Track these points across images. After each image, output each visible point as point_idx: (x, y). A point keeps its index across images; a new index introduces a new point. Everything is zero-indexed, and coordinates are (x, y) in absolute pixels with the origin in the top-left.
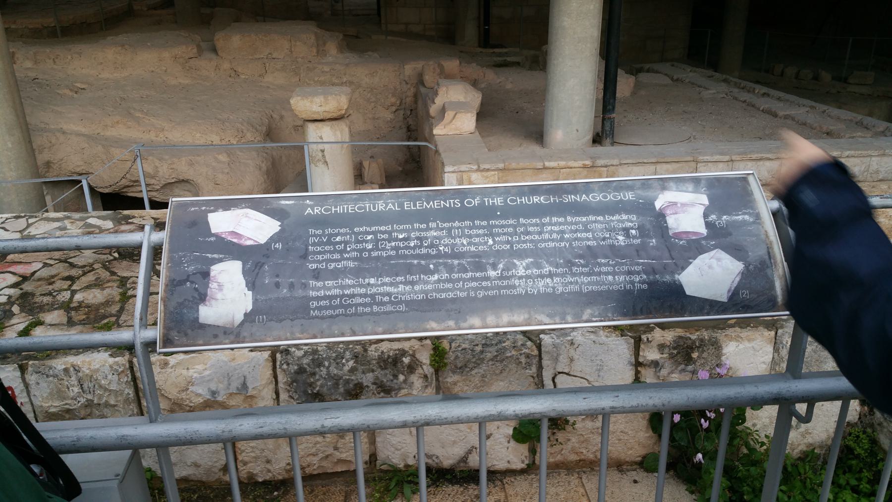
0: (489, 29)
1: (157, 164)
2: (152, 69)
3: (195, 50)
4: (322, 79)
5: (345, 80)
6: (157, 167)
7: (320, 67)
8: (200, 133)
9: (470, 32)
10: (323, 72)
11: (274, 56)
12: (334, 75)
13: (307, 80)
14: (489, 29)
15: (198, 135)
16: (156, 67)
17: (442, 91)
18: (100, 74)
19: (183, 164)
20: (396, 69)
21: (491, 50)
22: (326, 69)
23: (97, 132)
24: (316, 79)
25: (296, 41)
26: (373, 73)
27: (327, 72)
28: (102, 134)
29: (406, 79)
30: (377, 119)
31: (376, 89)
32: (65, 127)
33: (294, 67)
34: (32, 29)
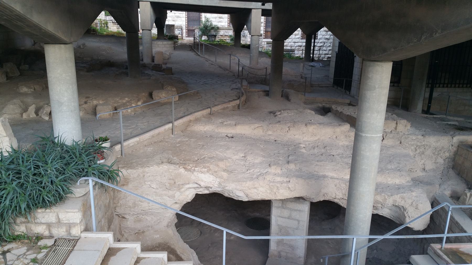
1: (386, 198)
2: (330, 136)
3: (349, 127)
4: (412, 143)
5: (424, 143)
6: (386, 199)
7: (411, 137)
8: (391, 178)
9: (420, 106)
10: (412, 139)
11: (386, 131)
12: (419, 141)
13: (405, 144)
14: (430, 106)
15: (390, 179)
16: (331, 136)
18: (304, 138)
19: (398, 197)
20: (449, 139)
21: (432, 116)
22: (414, 138)
23: (342, 177)
24: (410, 143)
25: (399, 124)
26: (438, 141)
27: (414, 140)
28: (344, 178)
29: (453, 144)
30: (437, 163)
31: (438, 148)
32: (327, 174)
33: (398, 137)
34: (233, 106)
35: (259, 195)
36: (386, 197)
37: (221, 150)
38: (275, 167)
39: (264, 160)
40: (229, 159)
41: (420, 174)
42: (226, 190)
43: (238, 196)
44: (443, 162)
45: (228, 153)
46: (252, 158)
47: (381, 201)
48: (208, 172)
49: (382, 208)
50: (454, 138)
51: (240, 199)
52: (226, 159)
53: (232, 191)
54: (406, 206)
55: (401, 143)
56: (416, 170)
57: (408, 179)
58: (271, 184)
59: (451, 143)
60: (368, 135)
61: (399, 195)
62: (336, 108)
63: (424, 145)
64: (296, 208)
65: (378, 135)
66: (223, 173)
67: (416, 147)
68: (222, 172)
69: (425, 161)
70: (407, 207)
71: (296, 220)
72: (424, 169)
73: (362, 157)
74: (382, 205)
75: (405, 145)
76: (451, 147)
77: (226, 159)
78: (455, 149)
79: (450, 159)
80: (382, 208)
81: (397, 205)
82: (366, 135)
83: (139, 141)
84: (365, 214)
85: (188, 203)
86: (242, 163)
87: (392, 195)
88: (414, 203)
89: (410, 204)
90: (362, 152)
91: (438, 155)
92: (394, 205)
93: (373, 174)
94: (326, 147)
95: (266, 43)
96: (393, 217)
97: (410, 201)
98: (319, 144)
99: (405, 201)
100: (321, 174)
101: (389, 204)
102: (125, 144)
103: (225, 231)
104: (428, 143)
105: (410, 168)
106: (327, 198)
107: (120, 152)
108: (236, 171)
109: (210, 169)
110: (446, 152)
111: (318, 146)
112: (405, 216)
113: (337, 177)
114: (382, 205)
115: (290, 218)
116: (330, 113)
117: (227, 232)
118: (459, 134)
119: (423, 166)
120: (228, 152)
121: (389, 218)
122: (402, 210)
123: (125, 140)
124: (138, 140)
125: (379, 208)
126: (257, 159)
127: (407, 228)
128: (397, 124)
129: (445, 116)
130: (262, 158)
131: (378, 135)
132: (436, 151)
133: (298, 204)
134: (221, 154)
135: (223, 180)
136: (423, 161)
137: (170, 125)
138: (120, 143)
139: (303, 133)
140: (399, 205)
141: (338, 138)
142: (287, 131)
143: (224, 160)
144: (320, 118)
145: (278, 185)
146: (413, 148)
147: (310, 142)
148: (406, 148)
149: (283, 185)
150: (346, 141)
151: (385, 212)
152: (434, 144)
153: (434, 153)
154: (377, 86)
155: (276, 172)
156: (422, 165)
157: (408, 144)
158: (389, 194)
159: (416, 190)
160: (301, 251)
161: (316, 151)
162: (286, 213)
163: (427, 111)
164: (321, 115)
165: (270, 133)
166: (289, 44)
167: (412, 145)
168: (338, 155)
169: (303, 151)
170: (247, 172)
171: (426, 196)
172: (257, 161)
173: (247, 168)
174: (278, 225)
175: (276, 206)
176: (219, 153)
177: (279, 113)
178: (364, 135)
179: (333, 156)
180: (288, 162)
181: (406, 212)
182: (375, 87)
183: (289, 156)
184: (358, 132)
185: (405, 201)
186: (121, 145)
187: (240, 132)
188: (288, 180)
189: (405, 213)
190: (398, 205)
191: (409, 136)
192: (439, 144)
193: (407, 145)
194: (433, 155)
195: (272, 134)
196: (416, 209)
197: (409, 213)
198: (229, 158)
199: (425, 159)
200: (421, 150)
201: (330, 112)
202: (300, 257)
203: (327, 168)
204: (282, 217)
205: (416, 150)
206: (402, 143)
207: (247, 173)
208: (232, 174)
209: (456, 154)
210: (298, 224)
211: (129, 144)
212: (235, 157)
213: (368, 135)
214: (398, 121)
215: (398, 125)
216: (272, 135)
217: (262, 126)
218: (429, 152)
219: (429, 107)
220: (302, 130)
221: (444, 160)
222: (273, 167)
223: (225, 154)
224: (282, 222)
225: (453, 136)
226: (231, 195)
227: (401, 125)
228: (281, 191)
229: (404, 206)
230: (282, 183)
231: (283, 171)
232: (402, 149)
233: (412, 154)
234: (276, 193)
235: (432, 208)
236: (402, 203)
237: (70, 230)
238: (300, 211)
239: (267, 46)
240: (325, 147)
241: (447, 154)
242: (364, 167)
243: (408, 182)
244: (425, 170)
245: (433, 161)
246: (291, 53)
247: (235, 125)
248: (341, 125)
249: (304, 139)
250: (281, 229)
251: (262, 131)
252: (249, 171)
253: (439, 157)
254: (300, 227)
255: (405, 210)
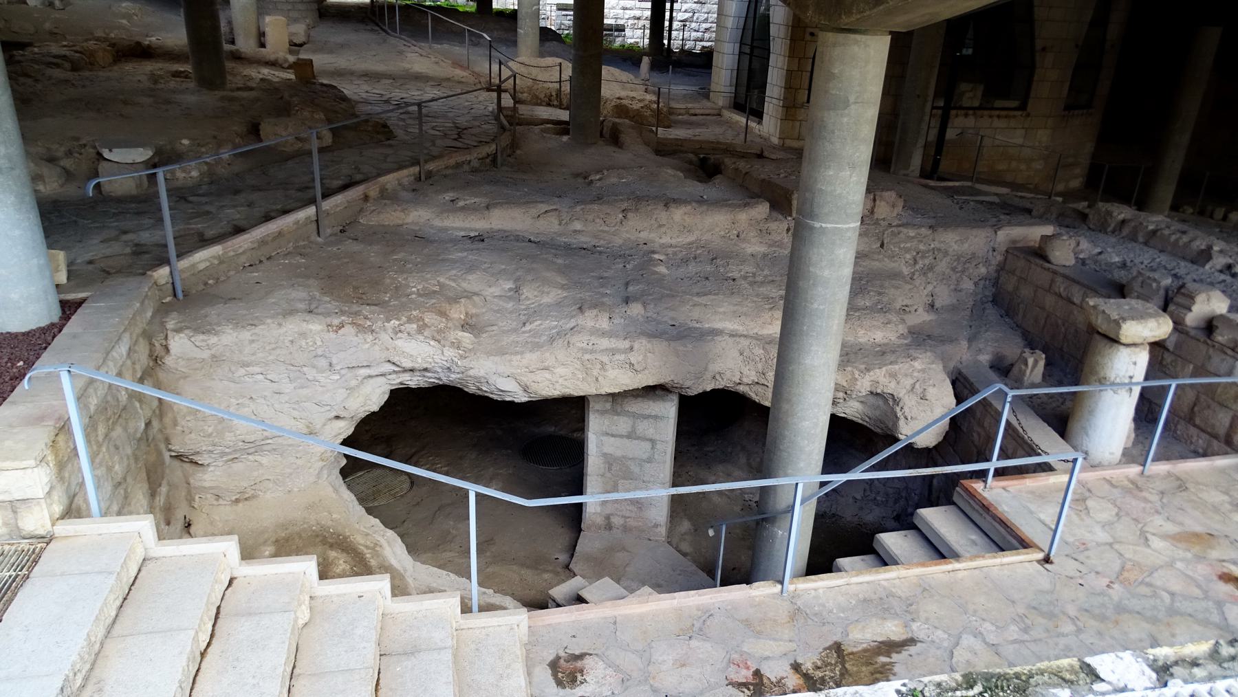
0: (940, 159)
1: (857, 376)
2: (723, 233)
4: (908, 245)
5: (932, 246)
6: (856, 379)
7: (904, 230)
10: (908, 237)
12: (922, 241)
14: (940, 159)
17: (1200, 299)
22: (912, 233)
24: (902, 246)
27: (913, 238)
30: (960, 291)
31: (963, 257)
32: (718, 325)
35: (557, 386)
36: (857, 373)
37: (454, 272)
38: (595, 312)
39: (566, 297)
40: (475, 298)
41: (922, 317)
42: (470, 377)
43: (502, 391)
44: (973, 287)
45: (473, 282)
46: (536, 293)
47: (845, 384)
48: (420, 331)
49: (845, 399)
50: (998, 233)
51: (508, 399)
52: (469, 295)
53: (485, 378)
54: (901, 393)
55: (882, 246)
56: (916, 307)
57: (902, 329)
58: (587, 356)
59: (992, 244)
60: (829, 226)
61: (884, 369)
62: (735, 163)
63: (933, 249)
64: (647, 412)
65: (852, 225)
66: (461, 334)
67: (915, 254)
68: (457, 332)
69: (935, 287)
70: (901, 395)
71: (647, 440)
72: (933, 306)
73: (811, 282)
74: (846, 393)
75: (892, 251)
76: (991, 253)
77: (469, 295)
78: (999, 258)
79: (987, 282)
80: (845, 399)
81: (879, 391)
82: (824, 225)
83: (222, 254)
84: (815, 420)
85: (373, 413)
86: (510, 305)
87: (868, 370)
88: (917, 386)
89: (909, 387)
90: (811, 269)
91: (963, 272)
92: (872, 393)
93: (836, 322)
94: (716, 258)
95: (555, 8)
96: (868, 420)
97: (908, 382)
98: (699, 252)
99: (898, 383)
100: (707, 326)
101: (863, 390)
102: (184, 264)
103: (473, 489)
104: (942, 245)
105: (904, 304)
106: (720, 385)
107: (170, 286)
108: (495, 328)
109: (425, 326)
110: (981, 265)
111: (695, 258)
112: (897, 417)
113: (745, 333)
114: (846, 393)
115: (631, 436)
116: (719, 176)
117: (478, 495)
118: (1010, 224)
119: (931, 299)
120: (470, 278)
121: (860, 422)
122: (891, 403)
123: (180, 256)
124: (221, 253)
125: (838, 400)
126: (548, 293)
127: (910, 447)
128: (874, 200)
129: (969, 184)
130: (560, 292)
131: (852, 225)
132: (958, 264)
133: (651, 403)
134: (453, 284)
135: (460, 352)
136: (930, 288)
137: (311, 211)
138: (165, 261)
139: (660, 226)
140: (885, 391)
141: (742, 236)
142: (618, 220)
143: (463, 300)
144: (695, 188)
145: (605, 359)
146: (908, 256)
147: (676, 247)
148: (894, 257)
149: (617, 357)
150: (761, 242)
151: (852, 410)
152: (956, 247)
153: (953, 269)
154: (852, 99)
155: (597, 326)
156: (927, 295)
157: (900, 248)
158: (863, 367)
159: (920, 356)
160: (660, 514)
161: (692, 268)
162: (622, 424)
163: (931, 171)
164: (700, 181)
165: (578, 226)
166: (612, 11)
167: (907, 250)
168: (745, 278)
169: (662, 269)
170: (524, 329)
171: (941, 367)
172: (546, 300)
173: (523, 318)
174: (605, 455)
175: (598, 411)
176: (448, 282)
177: (598, 177)
178: (817, 225)
179: (734, 280)
180: (627, 301)
181: (900, 406)
182: (848, 101)
183: (627, 284)
184: (803, 217)
185: (898, 383)
186: (171, 267)
187: (500, 227)
188: (627, 344)
189: (898, 409)
190: (882, 391)
191: (901, 229)
192: (966, 245)
193: (897, 249)
194: (952, 273)
195: (584, 229)
196: (921, 399)
197: (906, 409)
198: (477, 294)
199: (935, 283)
200: (927, 262)
201: (720, 173)
202: (656, 526)
203: (721, 310)
204: (613, 436)
205: (916, 262)
206: (885, 245)
207: (524, 332)
208: (484, 335)
209: (1001, 268)
210: (653, 448)
211: (193, 266)
212: (492, 290)
213: (829, 226)
214: (878, 193)
215: (878, 202)
216: (583, 231)
217: (556, 210)
218: (943, 266)
219: (936, 163)
220: (656, 219)
221: (976, 284)
222: (590, 314)
223: (464, 285)
224: (614, 446)
225: (996, 227)
226: (484, 389)
227: (883, 203)
228: (612, 373)
229: (895, 394)
230: (614, 351)
231: (615, 321)
232: (886, 259)
233: (906, 271)
234: (599, 379)
235: (960, 400)
236: (890, 387)
237: (16, 520)
238: (656, 417)
239: (557, 16)
240: (712, 260)
241: (983, 270)
242: (815, 306)
243: (902, 336)
244: (935, 307)
245: (952, 287)
246: (616, 33)
247: (488, 207)
248: (749, 204)
249: (663, 241)
250: (612, 465)
251: (556, 222)
252: (528, 327)
253: (965, 278)
254: (656, 457)
255: (896, 401)
